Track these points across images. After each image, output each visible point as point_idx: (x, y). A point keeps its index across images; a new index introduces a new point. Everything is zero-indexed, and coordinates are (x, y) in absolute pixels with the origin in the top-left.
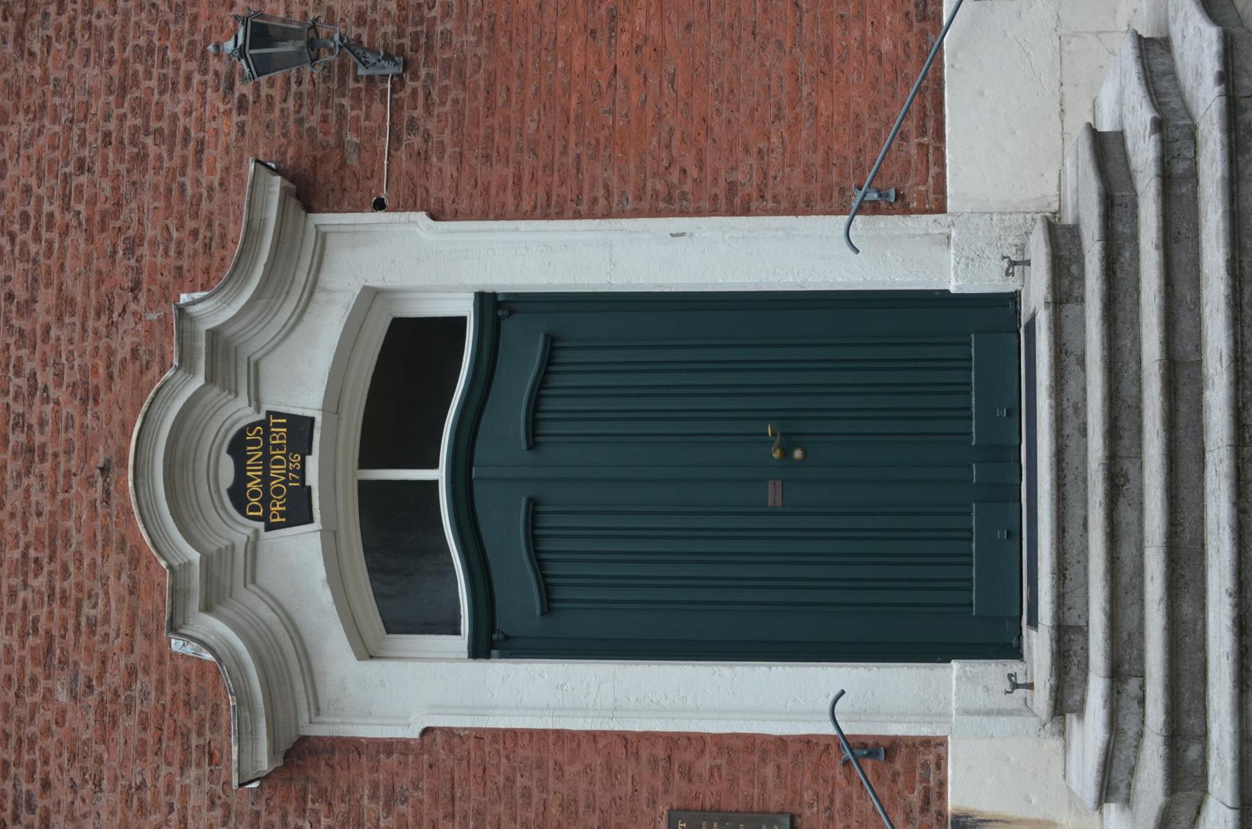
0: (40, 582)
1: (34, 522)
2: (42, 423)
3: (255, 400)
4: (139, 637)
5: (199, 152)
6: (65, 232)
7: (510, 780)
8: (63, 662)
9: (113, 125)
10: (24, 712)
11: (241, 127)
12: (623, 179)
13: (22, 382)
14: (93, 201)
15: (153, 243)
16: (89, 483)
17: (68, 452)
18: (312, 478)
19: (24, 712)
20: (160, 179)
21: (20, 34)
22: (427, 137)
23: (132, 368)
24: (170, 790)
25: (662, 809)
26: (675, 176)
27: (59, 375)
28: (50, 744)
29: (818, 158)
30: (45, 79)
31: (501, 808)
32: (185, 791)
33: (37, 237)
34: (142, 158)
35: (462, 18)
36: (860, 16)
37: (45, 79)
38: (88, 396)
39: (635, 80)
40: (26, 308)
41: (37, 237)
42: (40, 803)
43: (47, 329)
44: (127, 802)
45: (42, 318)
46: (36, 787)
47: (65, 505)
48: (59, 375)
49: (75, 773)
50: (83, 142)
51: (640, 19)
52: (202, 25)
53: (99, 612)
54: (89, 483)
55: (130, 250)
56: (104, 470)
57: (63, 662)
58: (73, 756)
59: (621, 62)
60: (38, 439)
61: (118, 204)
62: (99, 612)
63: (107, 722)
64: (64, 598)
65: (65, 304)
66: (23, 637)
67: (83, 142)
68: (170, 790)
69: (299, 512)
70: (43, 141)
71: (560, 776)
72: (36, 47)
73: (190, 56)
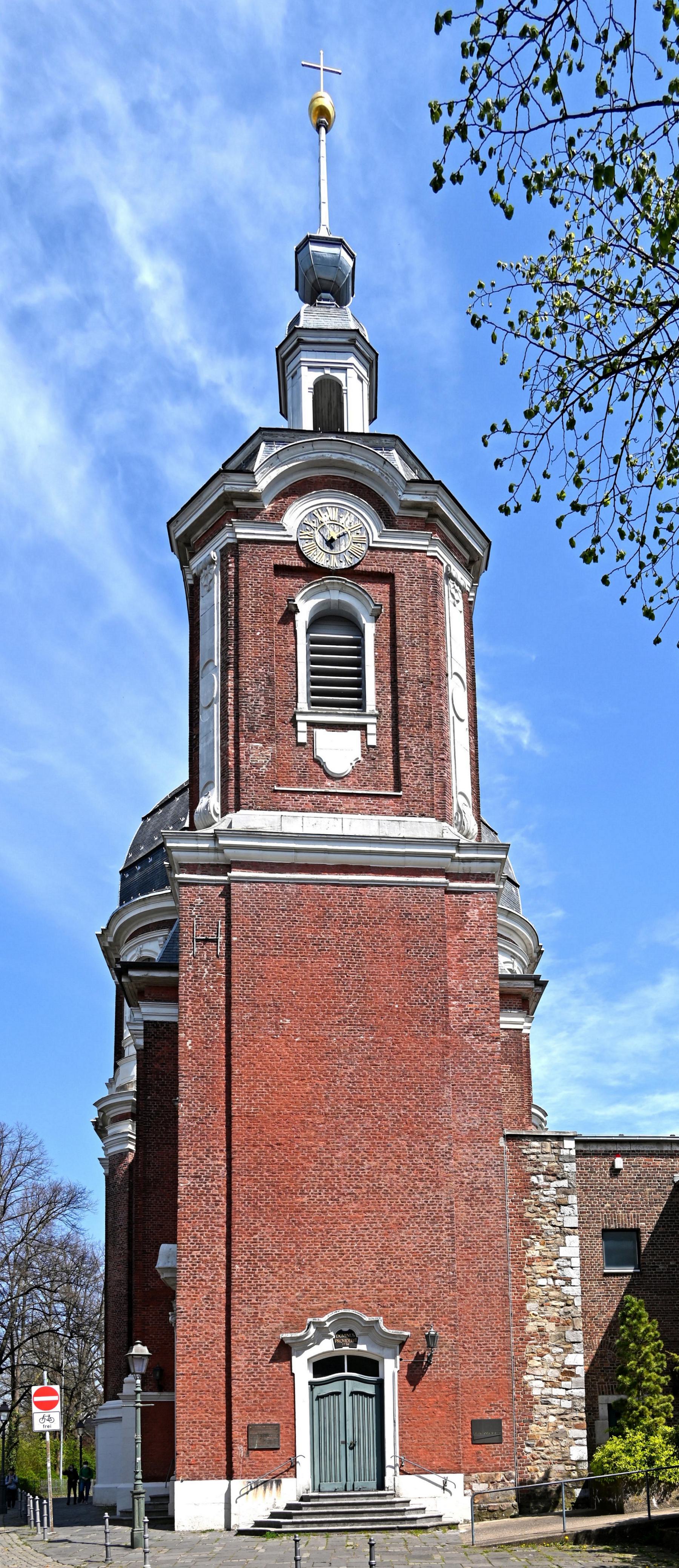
0: (321, 1288)
1: (333, 1286)
2: (355, 1287)
3: (361, 1335)
4: (310, 1311)
5: (413, 1320)
6: (396, 1290)
7: (284, 1391)
8: (304, 1294)
9: (419, 1299)
10: (293, 1285)
11: (417, 1329)
12: (406, 1410)
13: (363, 1282)
14: (402, 1296)
15: (393, 1310)
16: (342, 1298)
17: (349, 1293)
18: (344, 1348)
19: (293, 1285)
20: (407, 1311)
21: (439, 1276)
22: (415, 1369)
23: (366, 1307)
24: (279, 1319)
25: (280, 1422)
26: (407, 1421)
27: (365, 1290)
28: (287, 1292)
29: (410, 1449)
30: (429, 1283)
31: (279, 1390)
32: (279, 1323)
33: (395, 1283)
34: (411, 1306)
35: (440, 1375)
36: (440, 1457)
37: (429, 1283)
38: (361, 1297)
39: (427, 1412)
40: (379, 1282)
41: (395, 1283)
42: (274, 1290)
43: (375, 1287)
44: (276, 1310)
45: (377, 1285)
46: (277, 1289)
47: (337, 1293)
48: (365, 1290)
49: (281, 1298)
50: (415, 1292)
51: (440, 1412)
52: (440, 1318)
53: (315, 1302)
54: (342, 1298)
55: (392, 1305)
56: (345, 1302)
57: (304, 1294)
58: (284, 1297)
59: (430, 1409)
60: (351, 1286)
61: (402, 1302)
62: (315, 1302)
63: (292, 1305)
64: (317, 1294)
65: (380, 1290)
66: (309, 1285)
67: (415, 1292)
68: (279, 1319)
69: (337, 1345)
70: (415, 1283)
71: (286, 1401)
72: (436, 1280)
73: (433, 1316)
